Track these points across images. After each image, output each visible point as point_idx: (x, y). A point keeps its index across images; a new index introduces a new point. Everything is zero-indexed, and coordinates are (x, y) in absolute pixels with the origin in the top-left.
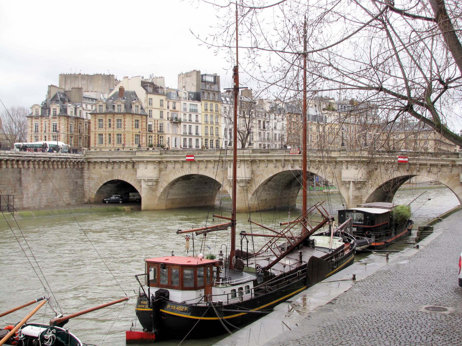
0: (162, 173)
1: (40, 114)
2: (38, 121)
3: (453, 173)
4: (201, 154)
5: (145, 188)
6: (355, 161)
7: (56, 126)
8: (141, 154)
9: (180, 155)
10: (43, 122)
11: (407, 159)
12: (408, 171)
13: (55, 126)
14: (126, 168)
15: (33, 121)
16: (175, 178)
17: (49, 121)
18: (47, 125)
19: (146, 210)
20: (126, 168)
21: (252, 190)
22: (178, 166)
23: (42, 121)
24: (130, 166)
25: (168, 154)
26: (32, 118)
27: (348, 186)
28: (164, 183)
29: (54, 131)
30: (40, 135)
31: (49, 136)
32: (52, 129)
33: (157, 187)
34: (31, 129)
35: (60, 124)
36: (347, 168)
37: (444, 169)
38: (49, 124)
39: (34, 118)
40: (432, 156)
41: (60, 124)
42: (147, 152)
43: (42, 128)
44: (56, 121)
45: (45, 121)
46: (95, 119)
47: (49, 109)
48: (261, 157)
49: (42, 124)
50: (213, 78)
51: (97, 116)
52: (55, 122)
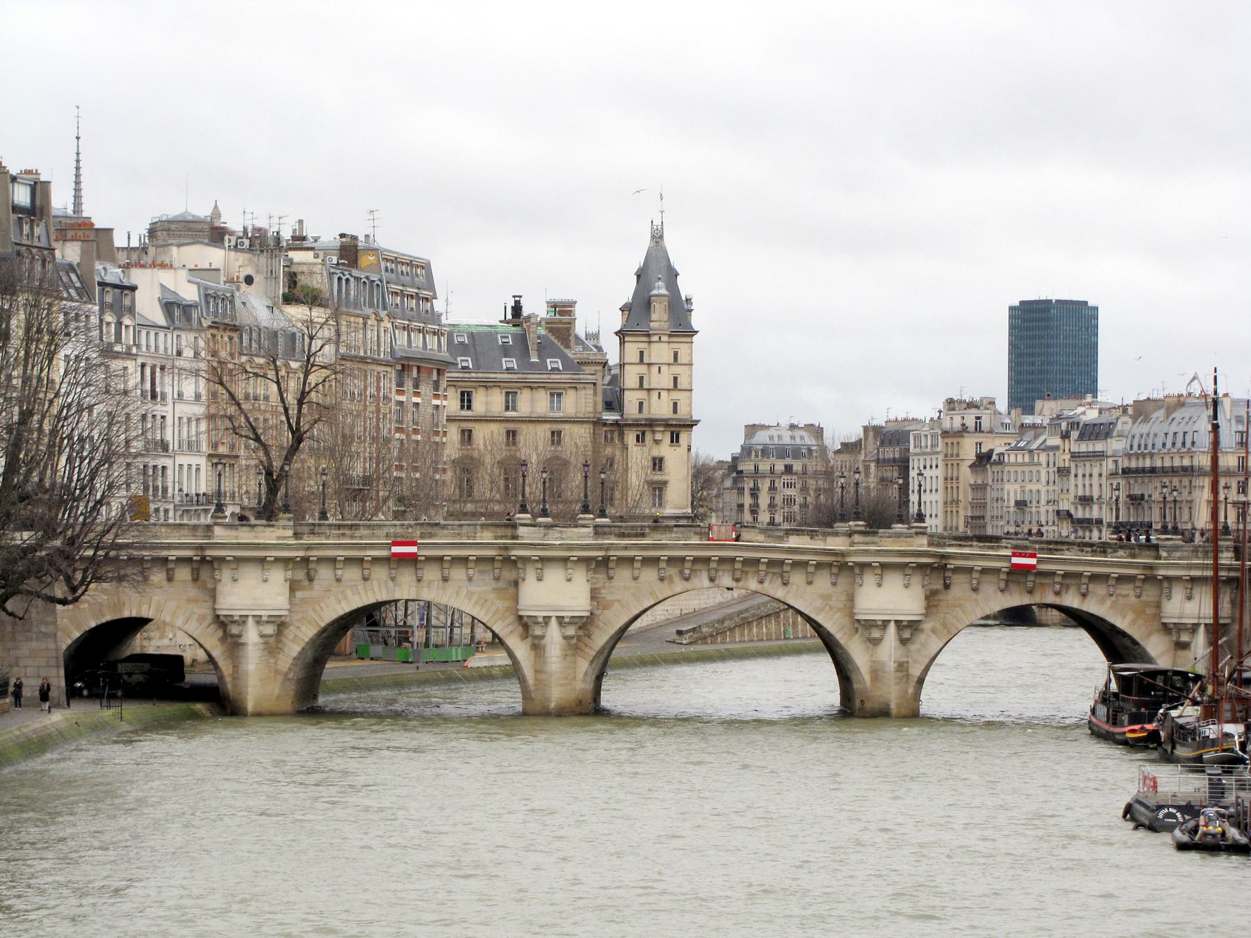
0: (299, 594)
3: (1144, 598)
4: (431, 536)
5: (256, 644)
6: (906, 565)
8: (251, 535)
9: (361, 538)
11: (1033, 561)
12: (1030, 592)
14: (170, 579)
16: (341, 613)
19: (258, 715)
20: (170, 579)
21: (591, 648)
22: (352, 574)
24: (183, 574)
25: (319, 534)
27: (876, 634)
28: (303, 628)
33: (279, 641)
36: (880, 585)
37: (1127, 589)
40: (1094, 553)
42: (271, 529)
48: (626, 548)
50: (28, 190)
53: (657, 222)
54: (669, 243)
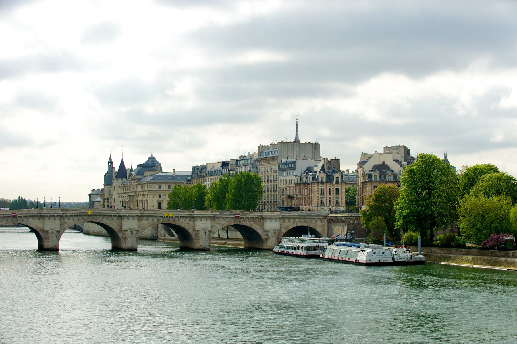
1: (325, 180)
2: (324, 186)
7: (338, 190)
10: (328, 187)
13: (337, 191)
15: (319, 186)
17: (333, 186)
18: (332, 189)
23: (326, 186)
26: (318, 184)
29: (336, 194)
30: (340, 197)
31: (333, 198)
32: (335, 192)
34: (317, 192)
35: (342, 188)
38: (333, 188)
41: (342, 188)
43: (327, 191)
44: (339, 187)
45: (329, 186)
46: (371, 185)
47: (333, 177)
49: (327, 188)
51: (373, 183)
52: (337, 187)
53: (445, 153)
54: (448, 157)
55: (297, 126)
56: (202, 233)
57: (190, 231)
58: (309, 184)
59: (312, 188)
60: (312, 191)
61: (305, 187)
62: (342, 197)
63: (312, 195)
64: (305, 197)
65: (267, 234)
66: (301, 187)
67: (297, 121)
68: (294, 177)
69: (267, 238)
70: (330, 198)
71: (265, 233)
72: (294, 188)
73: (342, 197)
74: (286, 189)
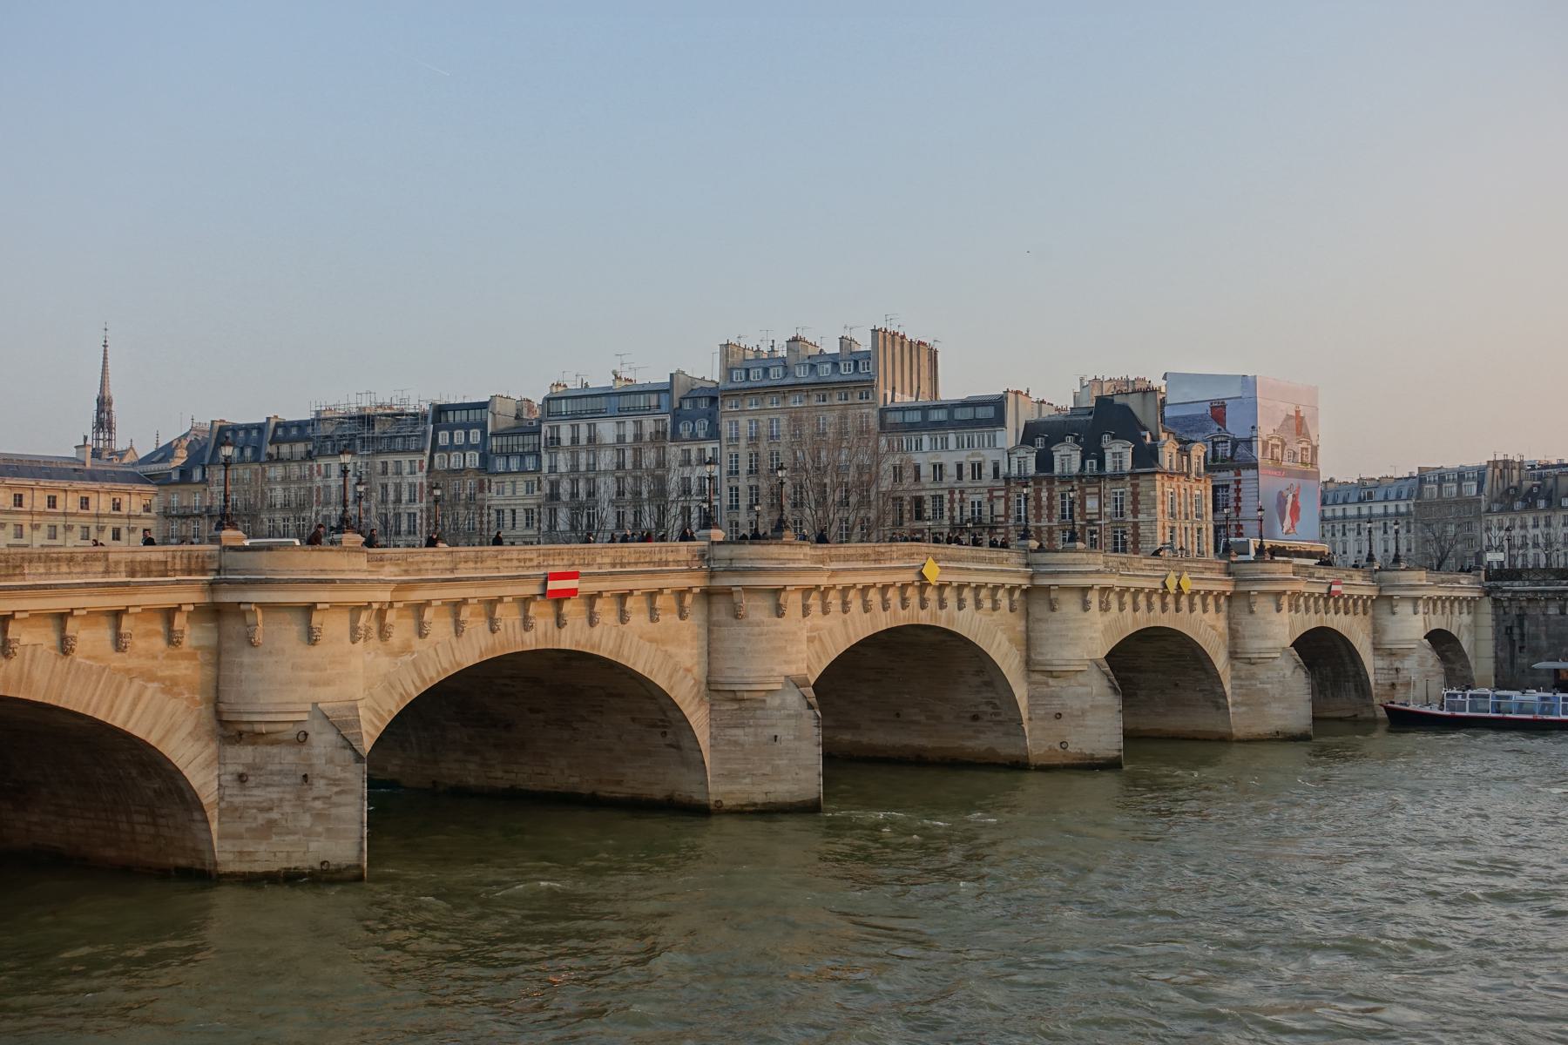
39: (1166, 478)
55: (105, 358)
56: (1288, 673)
57: (1220, 662)
58: (1117, 477)
59: (1135, 495)
60: (1135, 502)
61: (1082, 489)
62: (1207, 529)
63: (1141, 517)
64: (1083, 527)
65: (1397, 664)
66: (1050, 491)
67: (105, 346)
68: (988, 457)
69: (1393, 685)
70: (1186, 528)
71: (1380, 664)
72: (996, 494)
73: (1207, 529)
74: (938, 499)
